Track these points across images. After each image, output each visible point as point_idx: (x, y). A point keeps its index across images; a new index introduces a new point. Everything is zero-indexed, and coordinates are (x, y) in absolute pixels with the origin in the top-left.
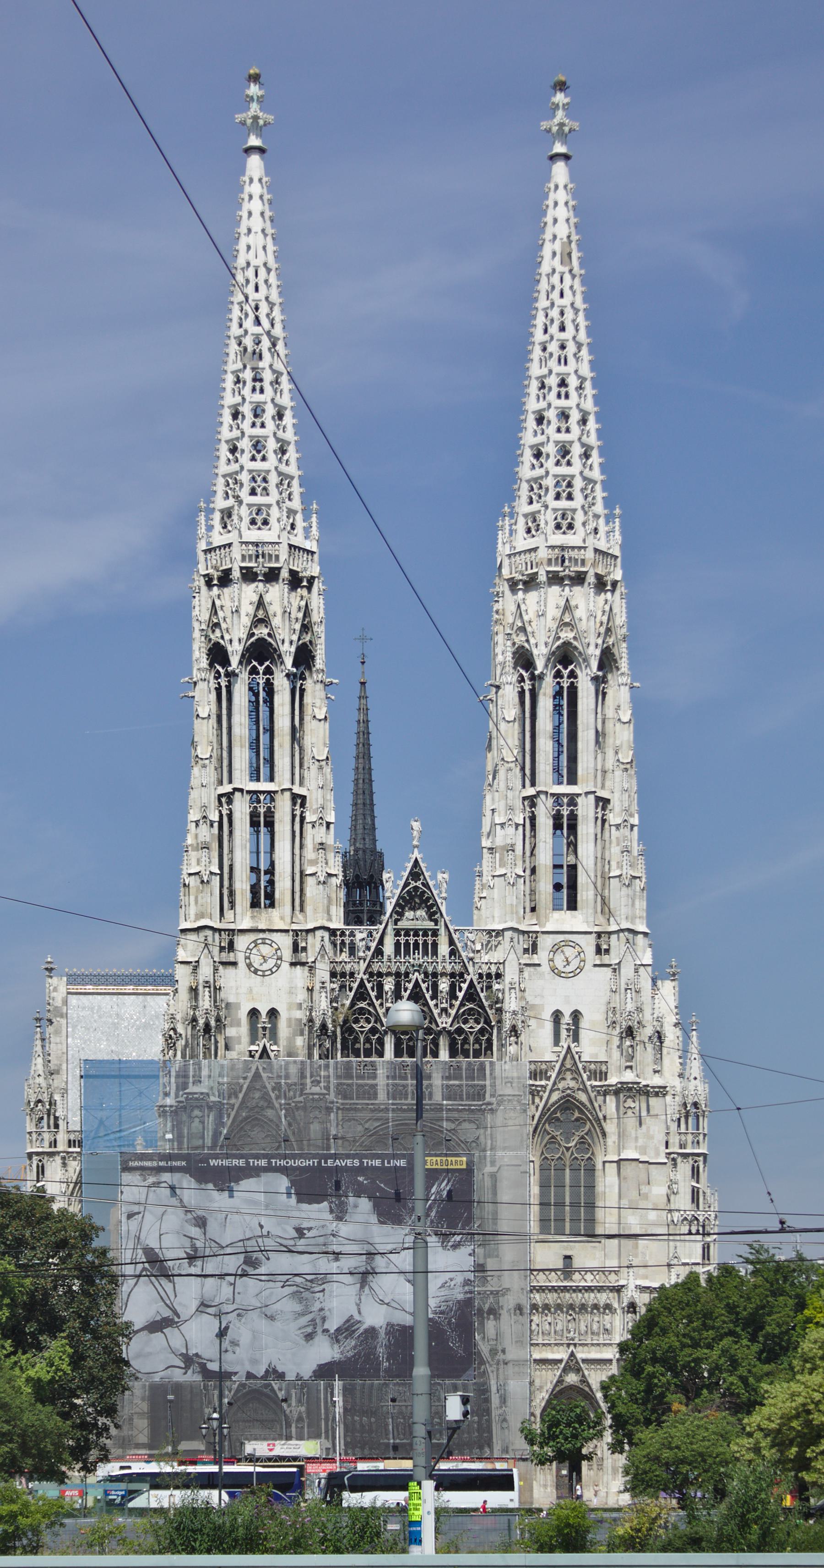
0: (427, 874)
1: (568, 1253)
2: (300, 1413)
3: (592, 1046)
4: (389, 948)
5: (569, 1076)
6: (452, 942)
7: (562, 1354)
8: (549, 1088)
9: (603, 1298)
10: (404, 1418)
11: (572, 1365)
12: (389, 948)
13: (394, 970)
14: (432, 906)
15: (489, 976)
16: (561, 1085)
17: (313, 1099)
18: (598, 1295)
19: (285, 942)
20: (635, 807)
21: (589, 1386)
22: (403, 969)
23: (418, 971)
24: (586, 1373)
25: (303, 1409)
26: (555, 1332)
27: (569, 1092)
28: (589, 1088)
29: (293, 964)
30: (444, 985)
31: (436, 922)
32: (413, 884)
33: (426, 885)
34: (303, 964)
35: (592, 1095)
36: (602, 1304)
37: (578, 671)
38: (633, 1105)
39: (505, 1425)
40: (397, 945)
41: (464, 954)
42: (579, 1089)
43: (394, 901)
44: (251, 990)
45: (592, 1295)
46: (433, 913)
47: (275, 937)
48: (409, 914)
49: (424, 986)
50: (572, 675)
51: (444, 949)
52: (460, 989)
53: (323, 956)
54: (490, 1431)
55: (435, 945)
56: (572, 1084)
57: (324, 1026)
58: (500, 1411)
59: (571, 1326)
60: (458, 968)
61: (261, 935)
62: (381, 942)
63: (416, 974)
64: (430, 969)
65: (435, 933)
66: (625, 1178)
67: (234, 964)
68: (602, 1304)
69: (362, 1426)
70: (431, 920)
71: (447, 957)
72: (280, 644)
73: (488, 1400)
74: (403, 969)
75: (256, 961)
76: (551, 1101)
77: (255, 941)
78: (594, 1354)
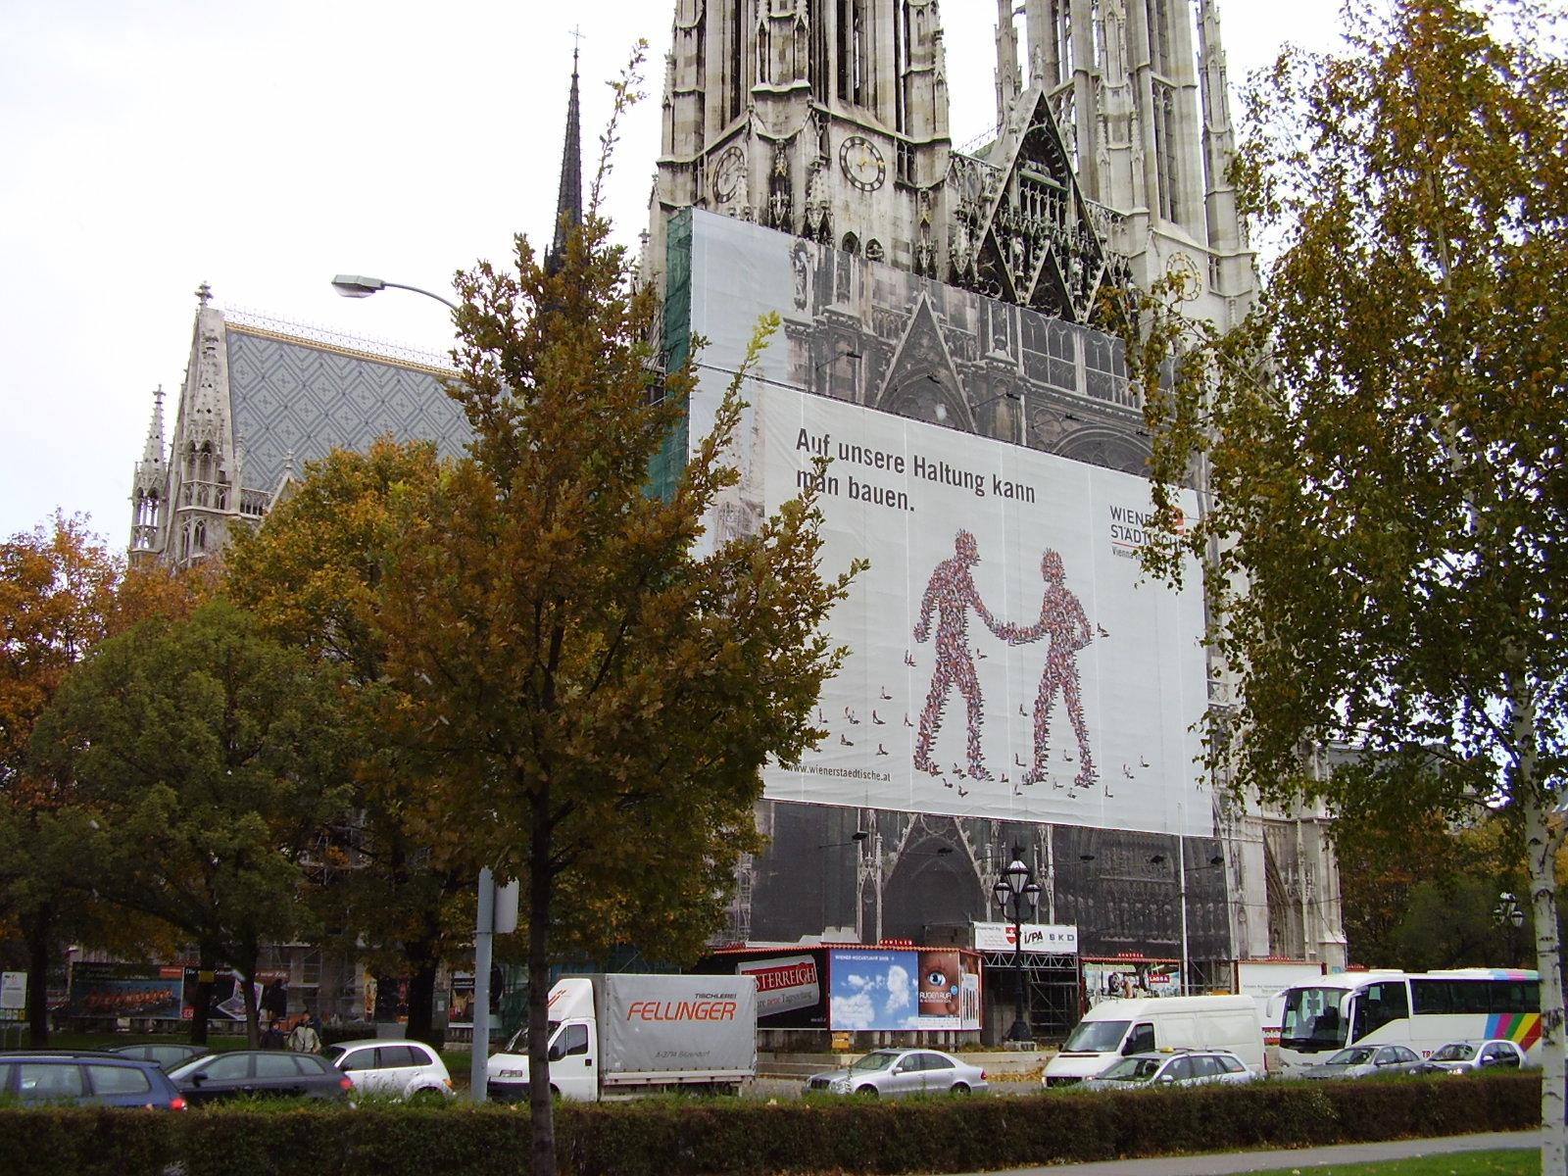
4: (1015, 200)
6: (1081, 213)
12: (1015, 200)
14: (1057, 159)
17: (997, 368)
19: (889, 153)
22: (1032, 232)
31: (1063, 183)
32: (1036, 126)
34: (913, 191)
40: (1023, 197)
44: (847, 207)
47: (877, 141)
48: (1034, 165)
51: (1072, 220)
52: (1094, 277)
53: (952, 180)
55: (1063, 213)
57: (969, 272)
61: (860, 135)
65: (1063, 197)
70: (1053, 176)
74: (1032, 232)
77: (852, 140)
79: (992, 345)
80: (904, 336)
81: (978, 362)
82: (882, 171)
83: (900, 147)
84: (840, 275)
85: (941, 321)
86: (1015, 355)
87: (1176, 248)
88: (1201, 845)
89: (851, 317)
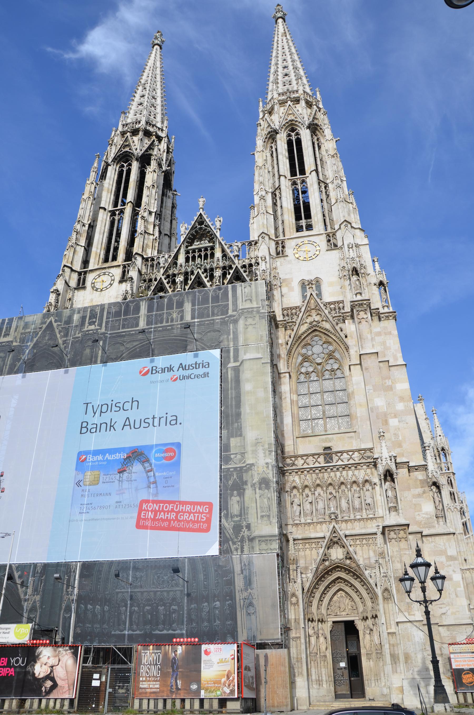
0: (207, 220)
1: (328, 445)
2: (35, 602)
3: (329, 294)
5: (314, 313)
6: (223, 251)
7: (324, 531)
8: (298, 322)
9: (361, 474)
10: (138, 606)
11: (334, 541)
13: (183, 270)
14: (212, 234)
15: (251, 265)
16: (308, 321)
18: (356, 472)
19: (117, 273)
20: (342, 173)
21: (355, 562)
23: (200, 268)
24: (351, 549)
25: (38, 598)
26: (317, 510)
27: (315, 323)
28: (331, 319)
29: (121, 282)
30: (218, 273)
33: (208, 226)
35: (334, 323)
36: (361, 481)
37: (301, 132)
38: (365, 316)
39: (251, 610)
40: (187, 260)
41: (231, 255)
42: (322, 321)
43: (185, 236)
45: (350, 473)
46: (212, 238)
49: (203, 276)
50: (298, 134)
51: (218, 254)
52: (229, 273)
54: (234, 618)
55: (212, 255)
56: (317, 318)
58: (245, 594)
59: (333, 504)
60: (227, 263)
61: (103, 271)
62: (176, 257)
63: (199, 270)
64: (208, 267)
65: (212, 248)
66: (366, 369)
67: (84, 288)
68: (361, 481)
69: (94, 615)
71: (220, 259)
72: (134, 151)
73: (231, 583)
74: (189, 270)
75: (98, 286)
76: (300, 332)
78: (358, 529)
79: (87, 324)
80: (35, 340)
81: (77, 335)
82: (114, 280)
83: (124, 267)
84: (7, 328)
85: (58, 325)
86: (100, 325)
87: (301, 240)
88: (200, 567)
89: (7, 342)
